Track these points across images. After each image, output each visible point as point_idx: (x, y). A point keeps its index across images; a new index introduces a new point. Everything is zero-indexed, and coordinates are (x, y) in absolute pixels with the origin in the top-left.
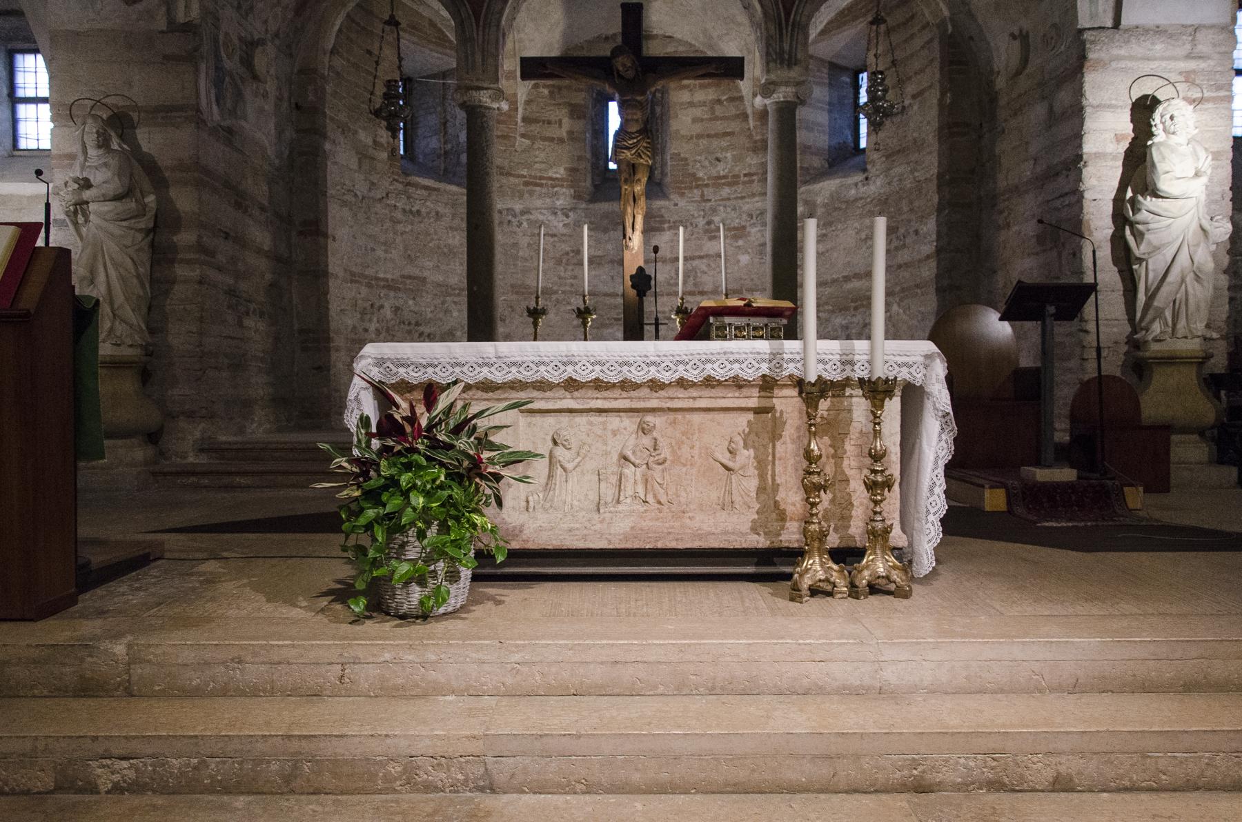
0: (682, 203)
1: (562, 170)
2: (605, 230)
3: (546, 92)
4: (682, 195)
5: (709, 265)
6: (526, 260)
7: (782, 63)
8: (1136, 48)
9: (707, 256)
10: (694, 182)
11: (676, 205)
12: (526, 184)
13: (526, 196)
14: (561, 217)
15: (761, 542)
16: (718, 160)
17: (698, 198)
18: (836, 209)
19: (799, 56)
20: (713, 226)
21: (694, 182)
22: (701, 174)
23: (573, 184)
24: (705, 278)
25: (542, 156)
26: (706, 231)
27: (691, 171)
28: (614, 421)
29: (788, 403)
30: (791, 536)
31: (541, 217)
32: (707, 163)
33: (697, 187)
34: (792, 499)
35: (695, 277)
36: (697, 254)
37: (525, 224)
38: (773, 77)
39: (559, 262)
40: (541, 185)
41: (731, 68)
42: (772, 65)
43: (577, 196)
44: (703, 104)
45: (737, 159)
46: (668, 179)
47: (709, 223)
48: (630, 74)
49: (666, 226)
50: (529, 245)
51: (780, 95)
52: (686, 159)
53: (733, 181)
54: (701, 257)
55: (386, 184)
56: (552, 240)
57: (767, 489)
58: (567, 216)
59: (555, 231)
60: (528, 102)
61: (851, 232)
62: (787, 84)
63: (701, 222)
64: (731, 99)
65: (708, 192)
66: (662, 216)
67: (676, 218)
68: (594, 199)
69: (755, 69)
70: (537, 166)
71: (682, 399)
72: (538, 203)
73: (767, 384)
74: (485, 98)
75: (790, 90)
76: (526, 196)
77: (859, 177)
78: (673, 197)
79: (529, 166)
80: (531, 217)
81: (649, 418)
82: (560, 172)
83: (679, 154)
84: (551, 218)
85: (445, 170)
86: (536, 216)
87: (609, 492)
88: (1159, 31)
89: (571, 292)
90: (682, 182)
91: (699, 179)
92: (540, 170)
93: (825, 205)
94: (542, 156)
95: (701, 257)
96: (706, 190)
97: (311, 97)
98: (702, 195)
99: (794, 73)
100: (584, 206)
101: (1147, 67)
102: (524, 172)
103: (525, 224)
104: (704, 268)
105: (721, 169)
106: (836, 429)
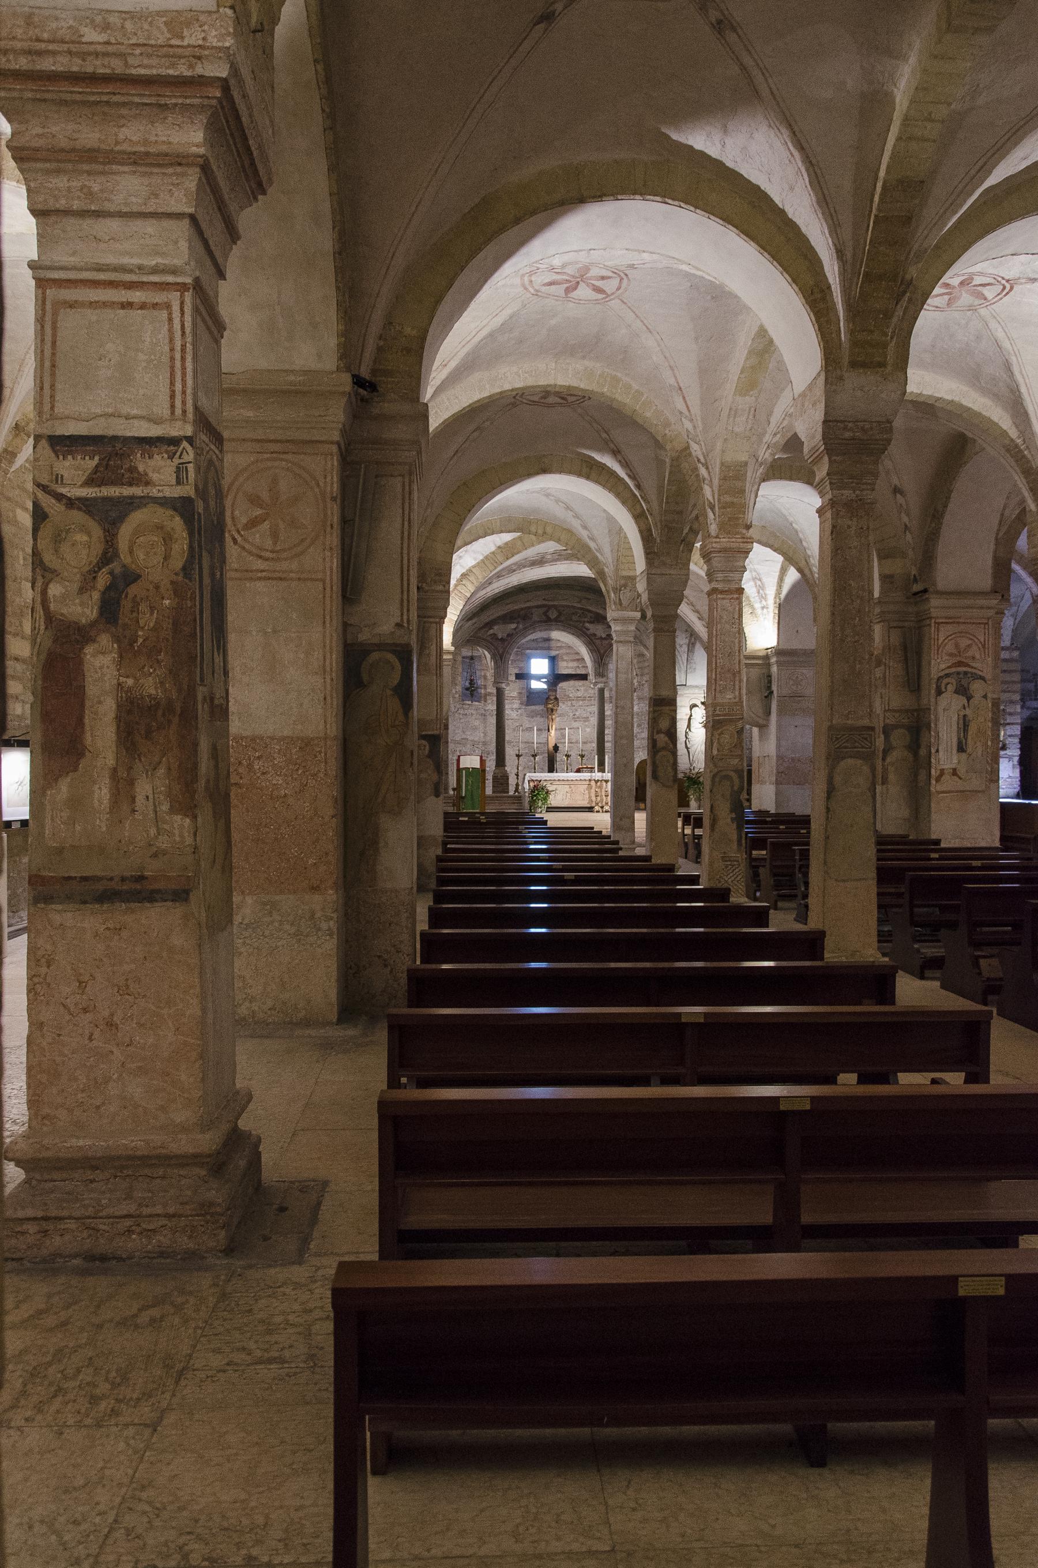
0: (563, 707)
2: (532, 717)
8: (691, 691)
10: (568, 698)
15: (589, 806)
21: (568, 698)
23: (520, 698)
24: (572, 737)
29: (593, 783)
30: (593, 805)
34: (594, 799)
39: (514, 730)
41: (584, 677)
43: (521, 704)
45: (586, 690)
51: (599, 686)
53: (584, 699)
55: (458, 706)
57: (590, 797)
63: (571, 714)
64: (583, 667)
65: (574, 702)
68: (527, 705)
69: (591, 677)
71: (576, 783)
73: (590, 780)
74: (503, 686)
82: (515, 694)
88: (697, 687)
99: (604, 680)
101: (694, 696)
105: (579, 694)
106: (601, 787)
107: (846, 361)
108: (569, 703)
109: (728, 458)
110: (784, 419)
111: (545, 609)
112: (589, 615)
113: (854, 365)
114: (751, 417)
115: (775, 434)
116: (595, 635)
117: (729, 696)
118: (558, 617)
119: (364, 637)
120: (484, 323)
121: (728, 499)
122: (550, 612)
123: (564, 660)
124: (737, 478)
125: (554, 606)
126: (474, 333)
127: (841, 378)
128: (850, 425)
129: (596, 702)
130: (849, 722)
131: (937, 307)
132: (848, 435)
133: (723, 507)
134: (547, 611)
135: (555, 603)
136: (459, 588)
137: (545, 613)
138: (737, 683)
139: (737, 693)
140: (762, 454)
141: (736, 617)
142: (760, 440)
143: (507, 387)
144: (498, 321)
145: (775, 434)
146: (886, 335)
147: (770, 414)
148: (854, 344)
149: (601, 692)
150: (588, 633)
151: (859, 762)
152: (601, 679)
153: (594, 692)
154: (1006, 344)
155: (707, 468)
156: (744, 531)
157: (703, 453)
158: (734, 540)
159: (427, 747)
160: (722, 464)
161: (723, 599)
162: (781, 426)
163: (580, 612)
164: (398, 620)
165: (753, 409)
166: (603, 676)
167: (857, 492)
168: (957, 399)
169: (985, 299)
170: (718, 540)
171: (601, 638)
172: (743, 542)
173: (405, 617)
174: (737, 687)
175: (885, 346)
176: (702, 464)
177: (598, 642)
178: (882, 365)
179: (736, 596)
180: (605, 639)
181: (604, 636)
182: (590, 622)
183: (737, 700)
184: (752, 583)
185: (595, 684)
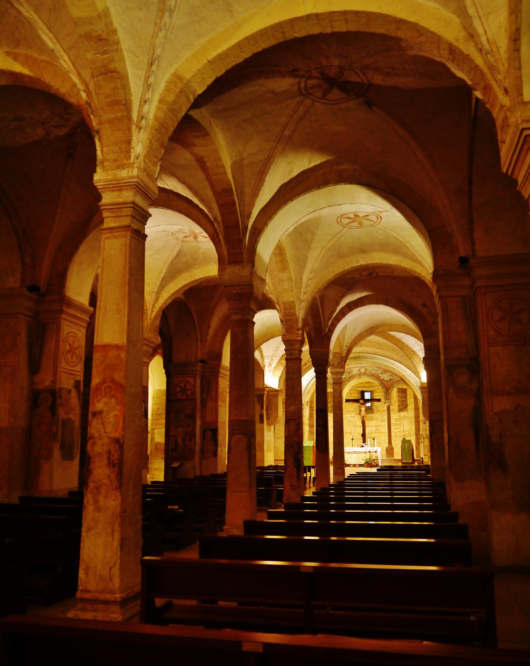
0: (377, 415)
1: (353, 409)
3: (350, 394)
4: (377, 413)
5: (382, 427)
6: (346, 427)
7: (387, 399)
9: (382, 426)
10: (379, 411)
11: (376, 415)
12: (346, 412)
13: (346, 414)
14: (353, 418)
16: (384, 407)
17: (380, 414)
18: (404, 418)
19: (390, 398)
20: (383, 420)
22: (380, 409)
25: (349, 407)
26: (382, 420)
27: (378, 408)
28: (355, 454)
31: (349, 418)
32: (381, 407)
33: (380, 412)
35: (380, 430)
36: (380, 425)
37: (346, 420)
38: (385, 402)
40: (348, 412)
42: (385, 400)
44: (380, 396)
46: (374, 410)
47: (382, 419)
48: (362, 403)
49: (374, 419)
50: (347, 424)
51: (387, 404)
52: (377, 406)
54: (381, 426)
56: (351, 422)
58: (354, 418)
59: (352, 421)
60: (346, 396)
61: (406, 423)
62: (388, 403)
63: (381, 419)
65: (382, 413)
66: (373, 417)
67: (376, 418)
70: (348, 408)
72: (348, 416)
75: (389, 404)
76: (346, 414)
77: (407, 413)
78: (375, 414)
79: (347, 409)
80: (347, 418)
81: (358, 454)
83: (376, 405)
84: (351, 418)
85: (331, 410)
86: (348, 418)
87: (355, 460)
89: (355, 433)
90: (377, 411)
91: (380, 410)
92: (349, 409)
93: (403, 417)
94: (349, 407)
95: (381, 426)
96: (381, 412)
97: (313, 406)
98: (381, 413)
99: (389, 401)
100: (357, 416)
102: (346, 410)
103: (346, 420)
104: (382, 428)
107: (227, 262)
108: (380, 413)
109: (285, 299)
110: (308, 281)
111: (359, 368)
112: (380, 370)
113: (230, 263)
114: (290, 281)
115: (306, 288)
116: (383, 380)
117: (293, 408)
118: (365, 372)
119: (40, 387)
120: (169, 254)
121: (288, 318)
122: (361, 369)
123: (376, 392)
124: (291, 308)
125: (364, 367)
126: (167, 259)
127: (224, 269)
128: (235, 287)
129: (386, 413)
130: (238, 418)
131: (357, 227)
132: (234, 292)
133: (286, 322)
134: (360, 369)
135: (363, 365)
136: (281, 361)
137: (359, 370)
138: (296, 401)
139: (296, 406)
140: (302, 296)
141: (296, 371)
142: (300, 292)
143: (197, 278)
144: (174, 254)
145: (306, 288)
146: (241, 249)
147: (302, 279)
148: (229, 254)
149: (389, 408)
150: (380, 378)
151: (242, 436)
152: (387, 401)
153: (385, 408)
154: (401, 239)
155: (279, 305)
156: (297, 332)
157: (276, 299)
158: (292, 336)
159: (211, 434)
160: (283, 303)
161: (290, 363)
162: (307, 285)
163: (376, 369)
164: (52, 380)
165: (290, 278)
166: (388, 400)
167: (243, 316)
168: (398, 264)
169: (374, 221)
170: (285, 336)
171: (387, 381)
172: (297, 337)
173: (55, 378)
174: (297, 404)
175: (242, 254)
176: (276, 303)
177: (385, 383)
178: (242, 262)
179: (296, 361)
180: (389, 381)
181: (388, 380)
182: (380, 373)
183: (296, 409)
184: (421, 352)
185: (385, 403)
